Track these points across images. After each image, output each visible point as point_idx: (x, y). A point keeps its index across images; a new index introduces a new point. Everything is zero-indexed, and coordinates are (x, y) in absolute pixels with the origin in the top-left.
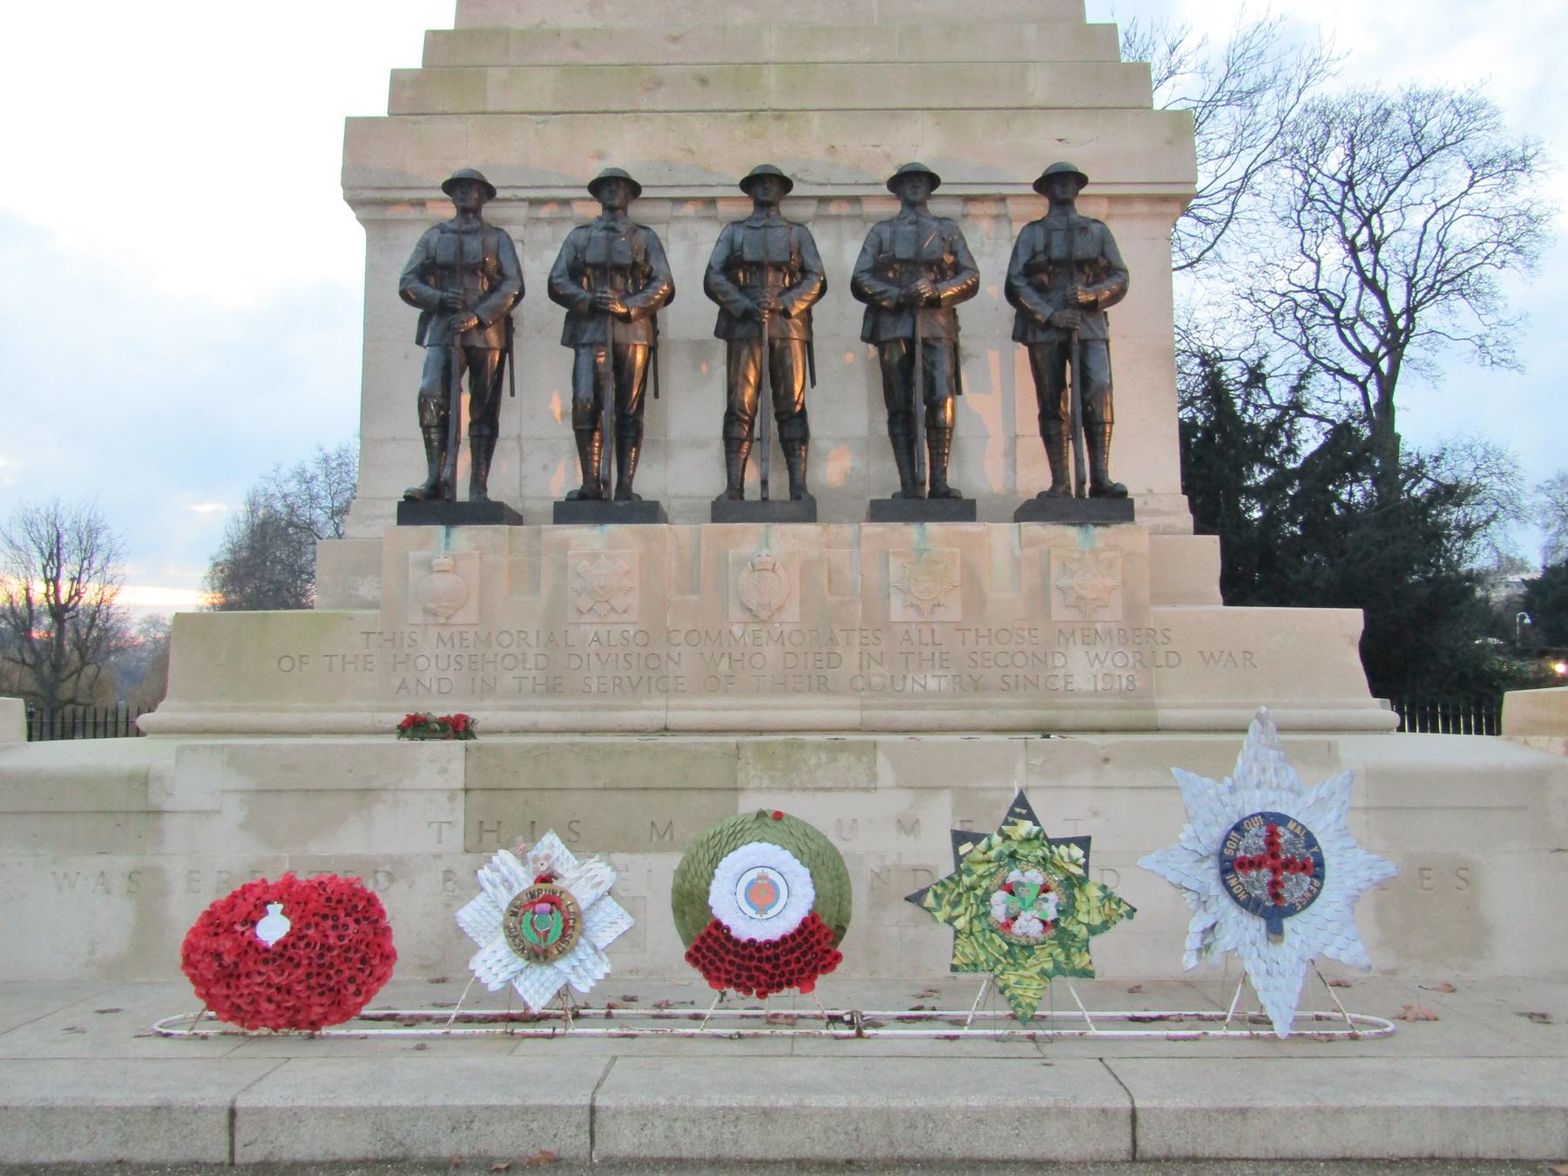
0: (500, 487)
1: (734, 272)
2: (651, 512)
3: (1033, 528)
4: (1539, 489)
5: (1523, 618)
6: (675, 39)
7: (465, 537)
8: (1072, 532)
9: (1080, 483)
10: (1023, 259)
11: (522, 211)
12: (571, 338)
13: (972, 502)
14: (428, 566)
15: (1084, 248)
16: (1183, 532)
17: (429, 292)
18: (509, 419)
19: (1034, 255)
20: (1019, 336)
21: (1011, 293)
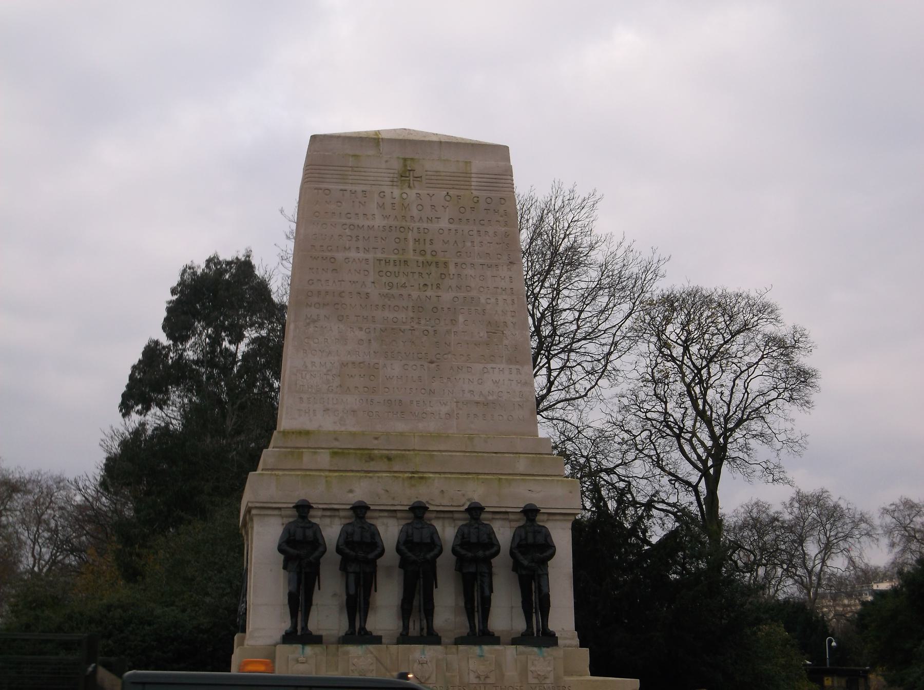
0: (312, 626)
1: (406, 544)
2: (377, 640)
3: (521, 648)
4: (886, 511)
5: (830, 642)
6: (376, 438)
7: (309, 650)
8: (535, 649)
9: (538, 631)
10: (517, 540)
11: (320, 513)
12: (344, 567)
13: (498, 638)
14: (297, 661)
15: (540, 539)
16: (575, 646)
17: (292, 551)
18: (317, 598)
19: (521, 540)
20: (515, 569)
21: (512, 553)
